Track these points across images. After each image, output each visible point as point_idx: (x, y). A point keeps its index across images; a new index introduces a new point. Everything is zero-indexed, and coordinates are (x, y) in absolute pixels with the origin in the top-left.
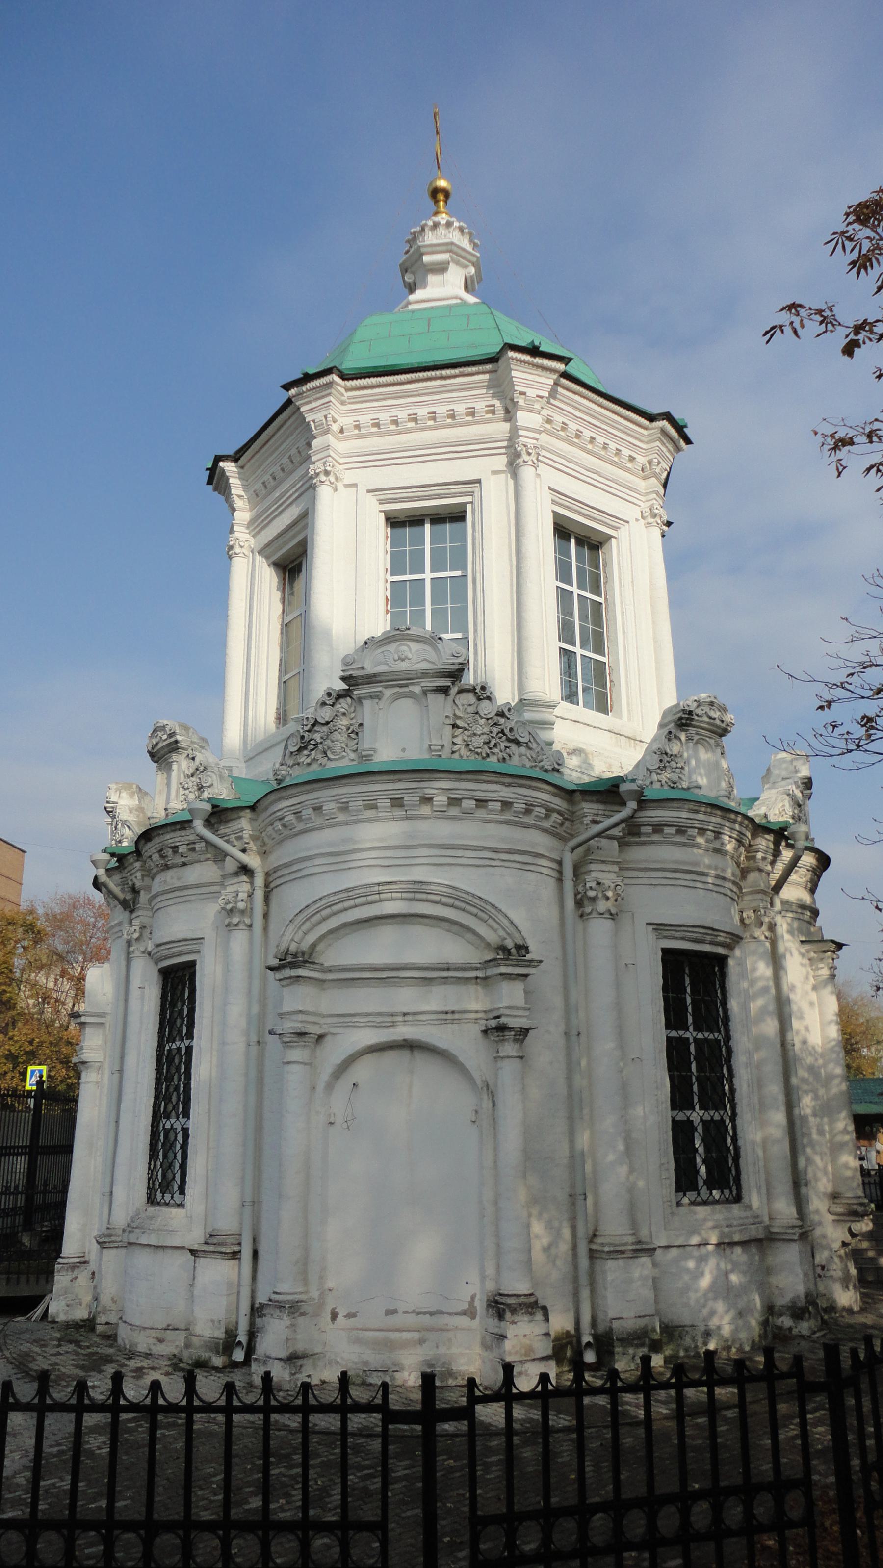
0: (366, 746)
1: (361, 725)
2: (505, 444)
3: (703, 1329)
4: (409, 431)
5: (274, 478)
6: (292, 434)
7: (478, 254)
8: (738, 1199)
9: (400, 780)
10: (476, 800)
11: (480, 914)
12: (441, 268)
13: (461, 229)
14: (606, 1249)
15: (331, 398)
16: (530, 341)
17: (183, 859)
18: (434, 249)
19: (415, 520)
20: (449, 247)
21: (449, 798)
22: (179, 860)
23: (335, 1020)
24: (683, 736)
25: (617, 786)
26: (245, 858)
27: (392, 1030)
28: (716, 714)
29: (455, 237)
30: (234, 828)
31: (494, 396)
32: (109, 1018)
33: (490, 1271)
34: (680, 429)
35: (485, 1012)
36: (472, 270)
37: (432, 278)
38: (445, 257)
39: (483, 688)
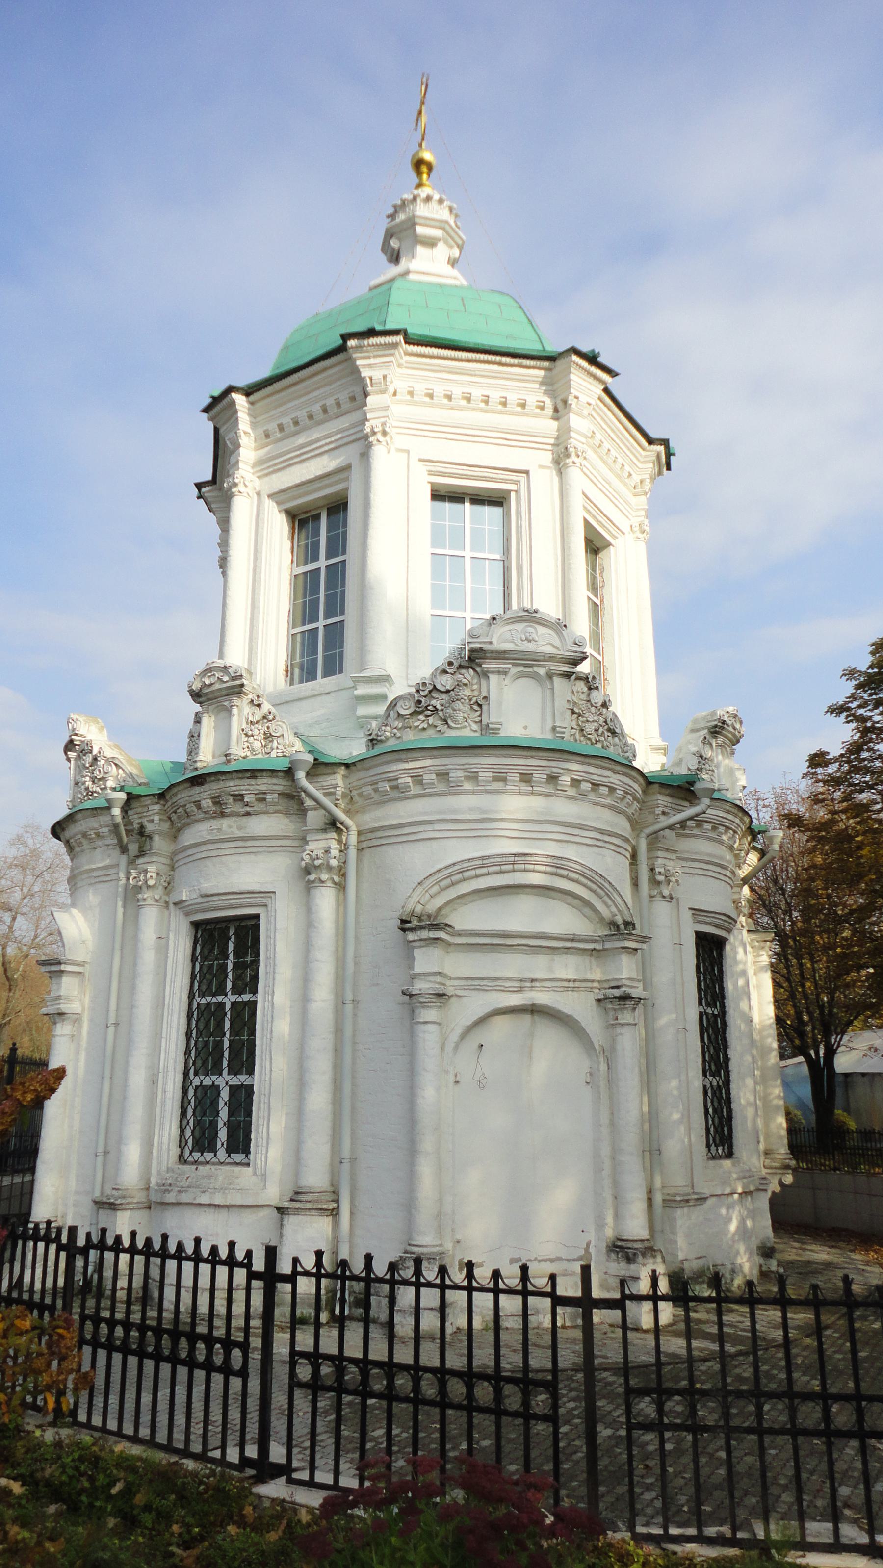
0: (492, 720)
1: (485, 698)
2: (552, 441)
3: (729, 1267)
4: (460, 408)
5: (296, 423)
6: (330, 383)
7: (464, 237)
8: (730, 1155)
9: (532, 757)
10: (593, 784)
11: (599, 890)
12: (431, 243)
13: (451, 209)
14: (678, 1198)
15: (391, 359)
16: (590, 348)
17: (248, 809)
18: (428, 222)
19: (454, 496)
20: (443, 225)
21: (572, 779)
22: (239, 808)
23: (462, 983)
24: (714, 744)
25: (692, 783)
26: (342, 816)
27: (520, 995)
28: (738, 726)
29: (445, 215)
30: (324, 784)
31: (546, 392)
32: (87, 966)
33: (610, 1220)
34: (669, 454)
35: (599, 981)
36: (456, 252)
37: (420, 250)
38: (438, 233)
39: (594, 678)
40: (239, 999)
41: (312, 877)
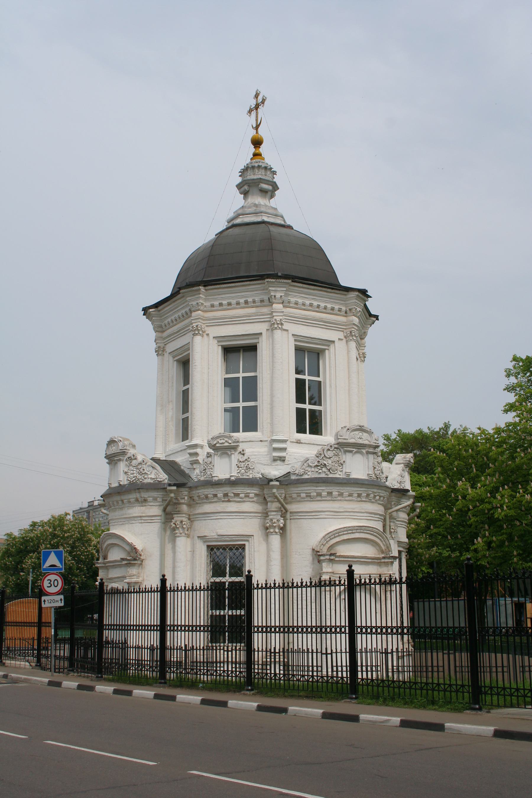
40: (221, 578)
41: (268, 531)
